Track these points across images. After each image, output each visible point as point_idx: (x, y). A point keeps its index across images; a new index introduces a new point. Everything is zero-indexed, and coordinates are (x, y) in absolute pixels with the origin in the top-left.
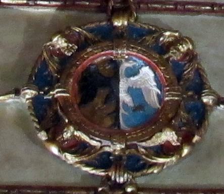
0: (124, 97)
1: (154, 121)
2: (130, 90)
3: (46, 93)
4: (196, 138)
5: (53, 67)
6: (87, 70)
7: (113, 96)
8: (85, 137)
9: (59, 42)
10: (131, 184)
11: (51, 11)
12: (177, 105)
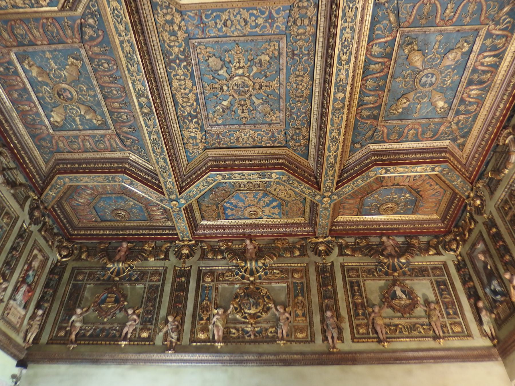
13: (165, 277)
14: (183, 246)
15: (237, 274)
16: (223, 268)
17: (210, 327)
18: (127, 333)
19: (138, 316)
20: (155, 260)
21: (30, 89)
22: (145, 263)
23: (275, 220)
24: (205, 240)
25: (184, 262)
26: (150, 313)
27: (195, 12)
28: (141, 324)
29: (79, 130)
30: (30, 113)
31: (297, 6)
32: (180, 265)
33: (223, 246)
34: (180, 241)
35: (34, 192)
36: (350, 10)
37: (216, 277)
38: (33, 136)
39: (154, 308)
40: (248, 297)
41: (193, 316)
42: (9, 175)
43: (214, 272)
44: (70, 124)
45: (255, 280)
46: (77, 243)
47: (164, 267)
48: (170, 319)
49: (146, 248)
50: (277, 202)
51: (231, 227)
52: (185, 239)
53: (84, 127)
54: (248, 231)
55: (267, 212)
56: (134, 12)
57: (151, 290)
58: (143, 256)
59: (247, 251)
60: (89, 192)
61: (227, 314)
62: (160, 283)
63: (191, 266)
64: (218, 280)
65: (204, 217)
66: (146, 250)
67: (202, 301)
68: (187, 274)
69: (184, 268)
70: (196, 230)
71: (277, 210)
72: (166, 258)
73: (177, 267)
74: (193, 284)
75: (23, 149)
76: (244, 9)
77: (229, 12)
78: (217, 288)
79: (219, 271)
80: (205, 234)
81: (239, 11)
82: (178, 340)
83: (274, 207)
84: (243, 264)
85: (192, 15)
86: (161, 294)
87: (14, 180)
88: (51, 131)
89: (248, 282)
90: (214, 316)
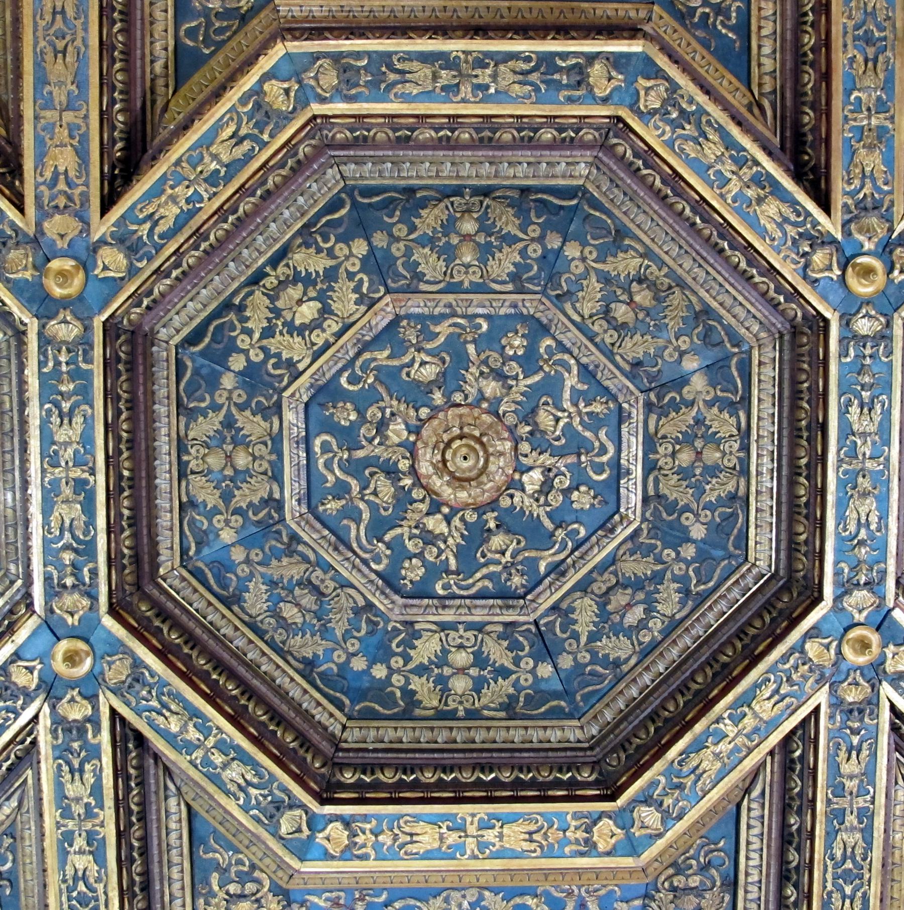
27: (334, 894)
31: (666, 885)
36: (848, 901)
56: (137, 889)
76: (495, 891)
77: (447, 900)
81: (481, 898)
85: (322, 904)
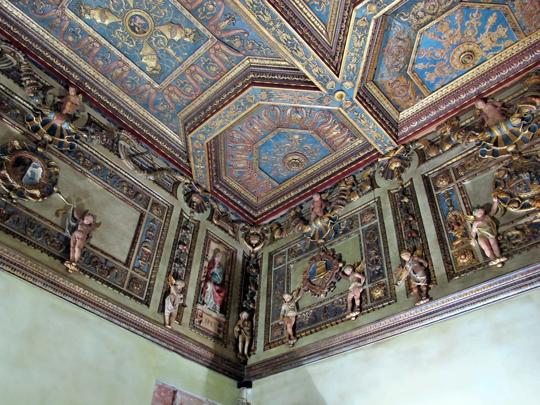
0: (29, 172)
1: (35, 186)
2: (31, 172)
3: (3, 156)
4: (46, 198)
5: (9, 149)
6: (21, 157)
7: (25, 170)
8: (8, 177)
9: (16, 143)
10: (16, 200)
11: (19, 133)
12: (45, 185)
13: (380, 210)
14: (389, 160)
15: (484, 153)
16: (460, 157)
17: (473, 243)
18: (353, 300)
19: (362, 273)
20: (360, 196)
21: (108, 44)
22: (349, 207)
23: (509, 50)
24: (417, 137)
25: (400, 178)
26: (377, 264)
28: (370, 282)
29: (181, 64)
30: (125, 75)
32: (393, 185)
33: (446, 132)
34: (383, 156)
35: (182, 175)
37: (453, 175)
38: (146, 106)
39: (380, 255)
40: (516, 173)
41: (439, 240)
42: (142, 162)
43: (448, 170)
44: (168, 63)
45: (517, 148)
46: (265, 225)
47: (375, 199)
48: (406, 257)
49: (343, 188)
50: (494, 14)
51: (445, 99)
52: (388, 150)
53: (183, 56)
54: (473, 91)
55: (488, 45)
57: (368, 235)
58: (343, 199)
59: (485, 119)
60: (241, 147)
61: (492, 213)
62: (377, 220)
63: (411, 180)
64: (458, 177)
65: (399, 106)
66: (345, 191)
67: (445, 217)
68: (408, 192)
69: (403, 186)
70: (397, 131)
71: (502, 31)
72: (374, 185)
73: (392, 190)
74: (423, 200)
75: (144, 126)
78: (461, 189)
79: (455, 165)
80: (413, 129)
82: (429, 281)
83: (493, 28)
84: (488, 135)
86: (384, 233)
87: (150, 165)
88: (157, 86)
89: (507, 155)
90: (472, 225)
